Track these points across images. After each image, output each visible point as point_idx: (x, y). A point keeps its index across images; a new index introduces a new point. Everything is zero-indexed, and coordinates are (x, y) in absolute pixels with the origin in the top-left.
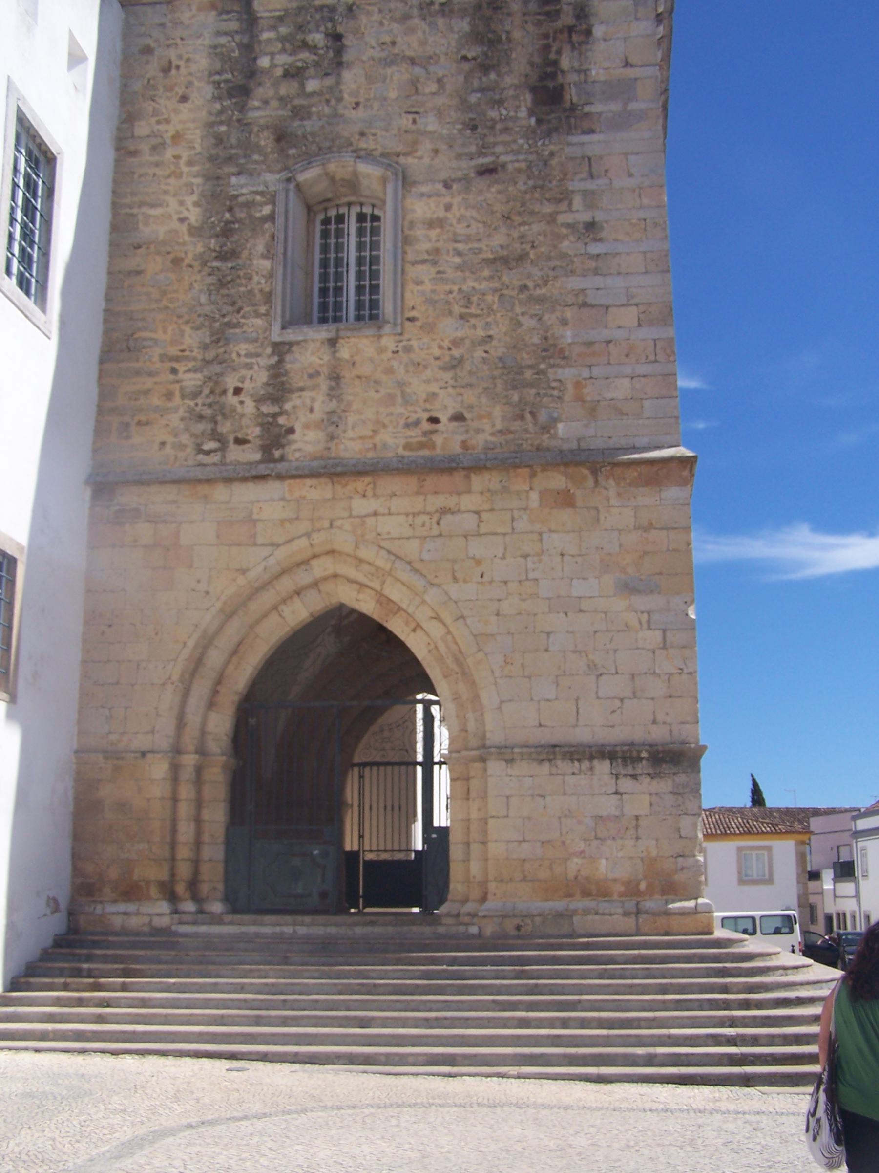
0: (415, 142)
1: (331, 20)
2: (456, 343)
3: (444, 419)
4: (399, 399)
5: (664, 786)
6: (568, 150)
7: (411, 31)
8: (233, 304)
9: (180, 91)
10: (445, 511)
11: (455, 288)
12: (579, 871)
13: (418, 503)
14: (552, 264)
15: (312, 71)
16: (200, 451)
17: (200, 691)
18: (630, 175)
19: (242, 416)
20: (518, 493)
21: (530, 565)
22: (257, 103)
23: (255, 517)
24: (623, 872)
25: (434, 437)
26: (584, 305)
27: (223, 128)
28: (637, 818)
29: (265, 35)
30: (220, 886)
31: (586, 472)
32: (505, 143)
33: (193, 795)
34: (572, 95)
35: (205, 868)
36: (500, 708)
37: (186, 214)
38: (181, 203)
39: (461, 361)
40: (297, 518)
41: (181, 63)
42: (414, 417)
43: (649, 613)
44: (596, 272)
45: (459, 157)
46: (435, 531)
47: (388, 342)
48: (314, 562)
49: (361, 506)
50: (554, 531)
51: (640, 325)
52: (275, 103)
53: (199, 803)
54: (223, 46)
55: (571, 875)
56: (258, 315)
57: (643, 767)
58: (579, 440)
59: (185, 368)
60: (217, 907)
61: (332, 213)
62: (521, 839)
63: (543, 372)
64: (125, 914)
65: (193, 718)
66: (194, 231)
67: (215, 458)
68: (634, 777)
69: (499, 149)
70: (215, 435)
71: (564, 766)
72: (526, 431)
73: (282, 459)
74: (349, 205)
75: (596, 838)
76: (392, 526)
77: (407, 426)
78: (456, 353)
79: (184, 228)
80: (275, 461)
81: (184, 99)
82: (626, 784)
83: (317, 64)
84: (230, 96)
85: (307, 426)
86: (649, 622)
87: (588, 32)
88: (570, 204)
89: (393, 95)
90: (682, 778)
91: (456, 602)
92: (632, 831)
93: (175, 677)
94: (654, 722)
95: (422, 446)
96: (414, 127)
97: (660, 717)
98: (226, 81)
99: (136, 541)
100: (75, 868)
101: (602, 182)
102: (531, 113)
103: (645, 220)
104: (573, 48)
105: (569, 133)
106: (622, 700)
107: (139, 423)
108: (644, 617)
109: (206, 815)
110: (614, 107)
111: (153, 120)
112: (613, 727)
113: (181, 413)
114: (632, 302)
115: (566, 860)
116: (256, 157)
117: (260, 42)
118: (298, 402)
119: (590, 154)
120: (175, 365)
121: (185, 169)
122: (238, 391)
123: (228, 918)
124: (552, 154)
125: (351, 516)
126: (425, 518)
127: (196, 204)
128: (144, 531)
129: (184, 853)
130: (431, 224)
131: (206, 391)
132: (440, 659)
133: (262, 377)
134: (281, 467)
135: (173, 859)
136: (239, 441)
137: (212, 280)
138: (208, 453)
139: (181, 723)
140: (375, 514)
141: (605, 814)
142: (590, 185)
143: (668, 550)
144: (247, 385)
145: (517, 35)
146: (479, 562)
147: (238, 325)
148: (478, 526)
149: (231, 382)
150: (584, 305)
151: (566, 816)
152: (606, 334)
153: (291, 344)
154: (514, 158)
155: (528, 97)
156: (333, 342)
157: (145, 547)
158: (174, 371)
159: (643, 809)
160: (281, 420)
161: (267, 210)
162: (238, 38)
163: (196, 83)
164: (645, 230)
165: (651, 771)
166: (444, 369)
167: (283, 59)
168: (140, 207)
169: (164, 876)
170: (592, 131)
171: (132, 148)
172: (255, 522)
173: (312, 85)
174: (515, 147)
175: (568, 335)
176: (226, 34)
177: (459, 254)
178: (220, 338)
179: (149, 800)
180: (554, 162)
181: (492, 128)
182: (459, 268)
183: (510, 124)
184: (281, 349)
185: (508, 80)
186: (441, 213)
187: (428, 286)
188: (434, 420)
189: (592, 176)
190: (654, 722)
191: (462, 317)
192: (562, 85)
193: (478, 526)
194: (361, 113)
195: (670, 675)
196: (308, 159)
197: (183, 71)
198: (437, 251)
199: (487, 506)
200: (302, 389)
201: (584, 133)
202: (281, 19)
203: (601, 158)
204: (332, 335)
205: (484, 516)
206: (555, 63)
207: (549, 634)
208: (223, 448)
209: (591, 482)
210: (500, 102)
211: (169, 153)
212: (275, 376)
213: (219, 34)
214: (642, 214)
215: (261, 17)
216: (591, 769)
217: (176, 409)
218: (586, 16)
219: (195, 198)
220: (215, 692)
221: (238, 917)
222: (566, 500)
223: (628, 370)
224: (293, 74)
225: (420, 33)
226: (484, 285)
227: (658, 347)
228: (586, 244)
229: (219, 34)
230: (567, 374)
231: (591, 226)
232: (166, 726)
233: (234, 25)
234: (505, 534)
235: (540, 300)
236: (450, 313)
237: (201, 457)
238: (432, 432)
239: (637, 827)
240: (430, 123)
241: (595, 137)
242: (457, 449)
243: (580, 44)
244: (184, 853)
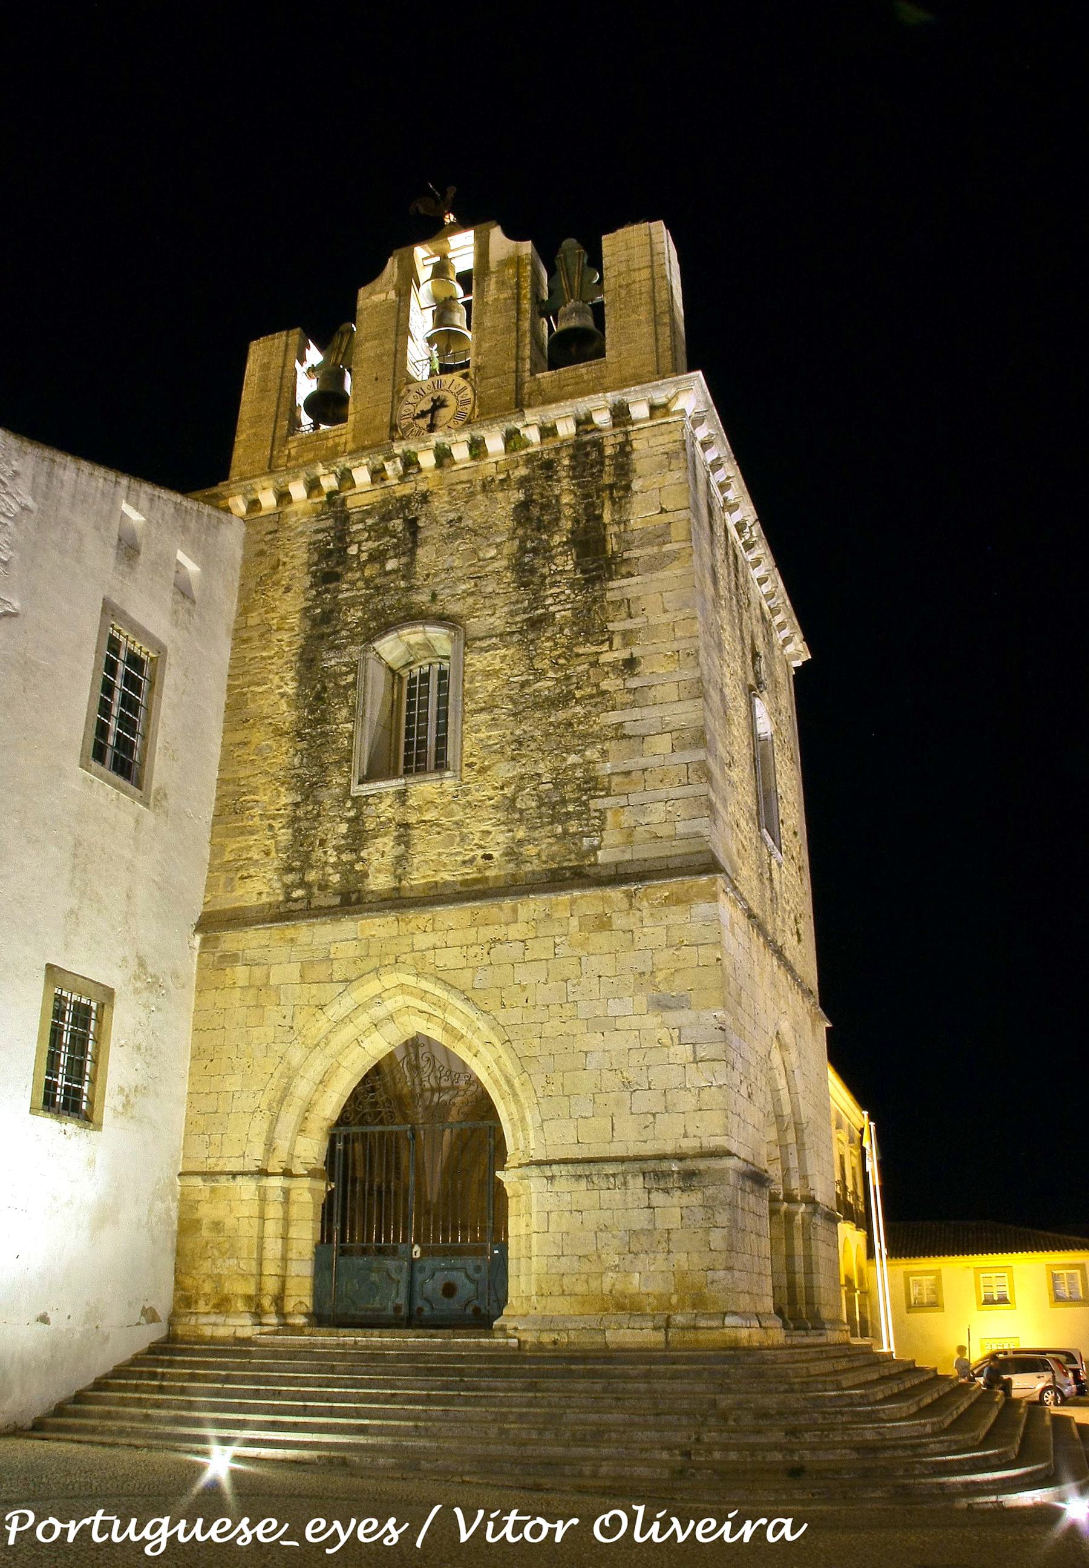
3: (495, 855)
5: (694, 1199)
11: (508, 732)
12: (614, 1285)
13: (471, 935)
15: (392, 553)
17: (290, 1117)
18: (665, 611)
20: (559, 920)
21: (570, 988)
23: (331, 956)
24: (657, 1286)
26: (625, 737)
28: (668, 1231)
29: (355, 528)
30: (308, 1301)
33: (280, 1214)
34: (612, 545)
35: (291, 1284)
36: (542, 1126)
40: (368, 955)
43: (679, 1029)
44: (633, 705)
46: (486, 961)
49: (422, 941)
50: (592, 954)
51: (673, 751)
52: (360, 584)
53: (287, 1222)
54: (321, 541)
55: (606, 1291)
58: (616, 866)
59: (280, 825)
62: (560, 1254)
64: (215, 1324)
65: (282, 1145)
68: (666, 1191)
69: (550, 601)
74: (430, 664)
75: (630, 1252)
76: (449, 958)
81: (288, 589)
82: (658, 1198)
83: (396, 546)
86: (679, 1037)
87: (628, 488)
88: (611, 644)
91: (503, 1027)
92: (664, 1245)
93: (263, 1107)
94: (685, 1136)
97: (691, 1130)
99: (234, 983)
100: (177, 1282)
103: (678, 651)
104: (614, 503)
105: (611, 579)
106: (654, 1115)
107: (242, 878)
109: (293, 1233)
112: (645, 1142)
114: (666, 730)
115: (602, 1274)
119: (629, 597)
120: (271, 821)
123: (307, 1330)
125: (413, 951)
126: (476, 949)
127: (293, 679)
128: (240, 973)
129: (271, 1268)
130: (488, 675)
132: (496, 1082)
135: (261, 1275)
138: (296, 900)
139: (270, 1147)
140: (434, 948)
141: (637, 1227)
142: (628, 625)
143: (698, 966)
145: (566, 499)
146: (524, 988)
148: (524, 954)
150: (625, 737)
151: (601, 1230)
152: (642, 762)
154: (561, 608)
159: (674, 1221)
161: (350, 678)
164: (678, 660)
165: (681, 1184)
168: (248, 687)
169: (251, 1290)
170: (630, 575)
171: (245, 636)
172: (332, 960)
173: (391, 565)
174: (563, 597)
179: (238, 1219)
183: (558, 578)
185: (557, 539)
189: (630, 616)
190: (685, 1136)
193: (524, 954)
195: (701, 1088)
197: (289, 567)
199: (532, 935)
201: (623, 577)
203: (638, 598)
205: (528, 943)
207: (586, 1053)
213: (317, 531)
214: (676, 646)
215: (352, 513)
216: (625, 1184)
218: (626, 474)
222: (603, 924)
223: (662, 795)
224: (378, 557)
227: (690, 770)
228: (624, 680)
229: (317, 531)
231: (631, 664)
234: (547, 960)
235: (584, 736)
239: (669, 1240)
241: (634, 580)
243: (620, 498)
244: (270, 1268)
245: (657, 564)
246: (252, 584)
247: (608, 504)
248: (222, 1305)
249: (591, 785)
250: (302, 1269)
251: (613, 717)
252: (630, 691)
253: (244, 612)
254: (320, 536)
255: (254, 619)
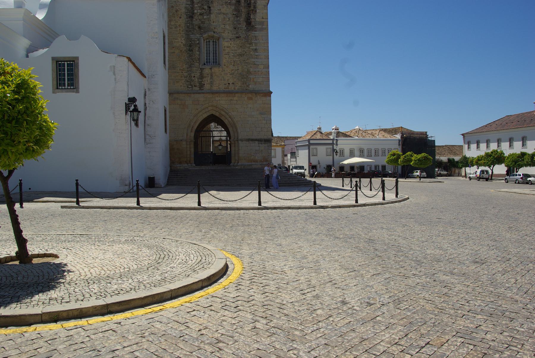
0: (225, 30)
1: (208, 4)
2: (232, 70)
3: (231, 84)
4: (223, 80)
5: (266, 145)
6: (252, 34)
7: (224, 8)
8: (192, 60)
9: (180, 16)
10: (231, 100)
14: (249, 56)
16: (188, 87)
18: (263, 40)
19: (195, 81)
22: (195, 20)
25: (229, 87)
27: (189, 24)
31: (254, 94)
32: (241, 32)
34: (253, 23)
37: (182, 41)
38: (181, 39)
39: (234, 73)
41: (180, 10)
42: (225, 83)
45: (232, 34)
47: (221, 69)
48: (209, 108)
49: (217, 99)
56: (197, 63)
57: (263, 142)
60: (194, 165)
61: (208, 40)
63: (247, 76)
66: (184, 45)
67: (191, 89)
69: (240, 33)
70: (191, 85)
71: (251, 142)
72: (245, 86)
73: (203, 90)
77: (224, 85)
78: (233, 72)
79: (182, 45)
80: (201, 90)
81: (180, 18)
82: (260, 145)
83: (206, 13)
84: (189, 18)
85: (207, 84)
87: (256, 11)
89: (220, 20)
90: (269, 144)
95: (227, 88)
96: (224, 27)
97: (266, 134)
98: (189, 15)
100: (170, 159)
101: (258, 41)
102: (246, 27)
107: (176, 82)
108: (263, 119)
110: (260, 26)
111: (175, 22)
113: (184, 80)
116: (195, 31)
117: (195, 7)
118: (205, 79)
121: (181, 32)
122: (194, 77)
123: (196, 167)
124: (249, 35)
130: (228, 47)
131: (188, 76)
133: (199, 74)
134: (203, 91)
136: (195, 86)
137: (188, 55)
138: (189, 88)
139: (187, 135)
142: (256, 42)
144: (196, 76)
145: (243, 10)
146: (237, 109)
147: (193, 64)
149: (193, 75)
153: (203, 68)
155: (245, 23)
156: (211, 69)
157: (180, 105)
158: (182, 72)
160: (202, 83)
161: (198, 42)
162: (190, 6)
163: (183, 15)
166: (230, 75)
167: (199, 11)
173: (205, 17)
175: (251, 70)
176: (188, 5)
177: (233, 53)
178: (190, 67)
180: (250, 36)
181: (239, 29)
182: (233, 56)
184: (202, 69)
185: (241, 19)
186: (230, 45)
187: (227, 59)
188: (229, 84)
191: (234, 65)
192: (251, 22)
194: (215, 24)
196: (205, 32)
198: (229, 52)
200: (206, 77)
202: (198, 2)
204: (211, 67)
206: (250, 17)
208: (192, 87)
209: (255, 96)
210: (240, 24)
211: (178, 29)
212: (201, 74)
213: (186, 4)
217: (183, 79)
219: (184, 38)
220: (192, 129)
221: (197, 166)
222: (251, 99)
225: (225, 8)
226: (237, 60)
229: (186, 4)
230: (251, 76)
231: (256, 49)
232: (185, 135)
233: (189, 3)
236: (231, 64)
237: (188, 89)
238: (229, 86)
240: (227, 27)
242: (233, 89)
245: (262, 29)
246: (171, 14)
247: (252, 14)
248: (180, 163)
249: (249, 72)
250: (193, 156)
251: (253, 60)
252: (256, 55)
253: (170, 21)
254: (187, 6)
255: (173, 23)
